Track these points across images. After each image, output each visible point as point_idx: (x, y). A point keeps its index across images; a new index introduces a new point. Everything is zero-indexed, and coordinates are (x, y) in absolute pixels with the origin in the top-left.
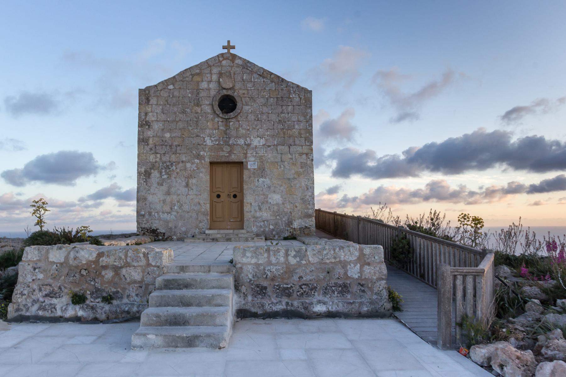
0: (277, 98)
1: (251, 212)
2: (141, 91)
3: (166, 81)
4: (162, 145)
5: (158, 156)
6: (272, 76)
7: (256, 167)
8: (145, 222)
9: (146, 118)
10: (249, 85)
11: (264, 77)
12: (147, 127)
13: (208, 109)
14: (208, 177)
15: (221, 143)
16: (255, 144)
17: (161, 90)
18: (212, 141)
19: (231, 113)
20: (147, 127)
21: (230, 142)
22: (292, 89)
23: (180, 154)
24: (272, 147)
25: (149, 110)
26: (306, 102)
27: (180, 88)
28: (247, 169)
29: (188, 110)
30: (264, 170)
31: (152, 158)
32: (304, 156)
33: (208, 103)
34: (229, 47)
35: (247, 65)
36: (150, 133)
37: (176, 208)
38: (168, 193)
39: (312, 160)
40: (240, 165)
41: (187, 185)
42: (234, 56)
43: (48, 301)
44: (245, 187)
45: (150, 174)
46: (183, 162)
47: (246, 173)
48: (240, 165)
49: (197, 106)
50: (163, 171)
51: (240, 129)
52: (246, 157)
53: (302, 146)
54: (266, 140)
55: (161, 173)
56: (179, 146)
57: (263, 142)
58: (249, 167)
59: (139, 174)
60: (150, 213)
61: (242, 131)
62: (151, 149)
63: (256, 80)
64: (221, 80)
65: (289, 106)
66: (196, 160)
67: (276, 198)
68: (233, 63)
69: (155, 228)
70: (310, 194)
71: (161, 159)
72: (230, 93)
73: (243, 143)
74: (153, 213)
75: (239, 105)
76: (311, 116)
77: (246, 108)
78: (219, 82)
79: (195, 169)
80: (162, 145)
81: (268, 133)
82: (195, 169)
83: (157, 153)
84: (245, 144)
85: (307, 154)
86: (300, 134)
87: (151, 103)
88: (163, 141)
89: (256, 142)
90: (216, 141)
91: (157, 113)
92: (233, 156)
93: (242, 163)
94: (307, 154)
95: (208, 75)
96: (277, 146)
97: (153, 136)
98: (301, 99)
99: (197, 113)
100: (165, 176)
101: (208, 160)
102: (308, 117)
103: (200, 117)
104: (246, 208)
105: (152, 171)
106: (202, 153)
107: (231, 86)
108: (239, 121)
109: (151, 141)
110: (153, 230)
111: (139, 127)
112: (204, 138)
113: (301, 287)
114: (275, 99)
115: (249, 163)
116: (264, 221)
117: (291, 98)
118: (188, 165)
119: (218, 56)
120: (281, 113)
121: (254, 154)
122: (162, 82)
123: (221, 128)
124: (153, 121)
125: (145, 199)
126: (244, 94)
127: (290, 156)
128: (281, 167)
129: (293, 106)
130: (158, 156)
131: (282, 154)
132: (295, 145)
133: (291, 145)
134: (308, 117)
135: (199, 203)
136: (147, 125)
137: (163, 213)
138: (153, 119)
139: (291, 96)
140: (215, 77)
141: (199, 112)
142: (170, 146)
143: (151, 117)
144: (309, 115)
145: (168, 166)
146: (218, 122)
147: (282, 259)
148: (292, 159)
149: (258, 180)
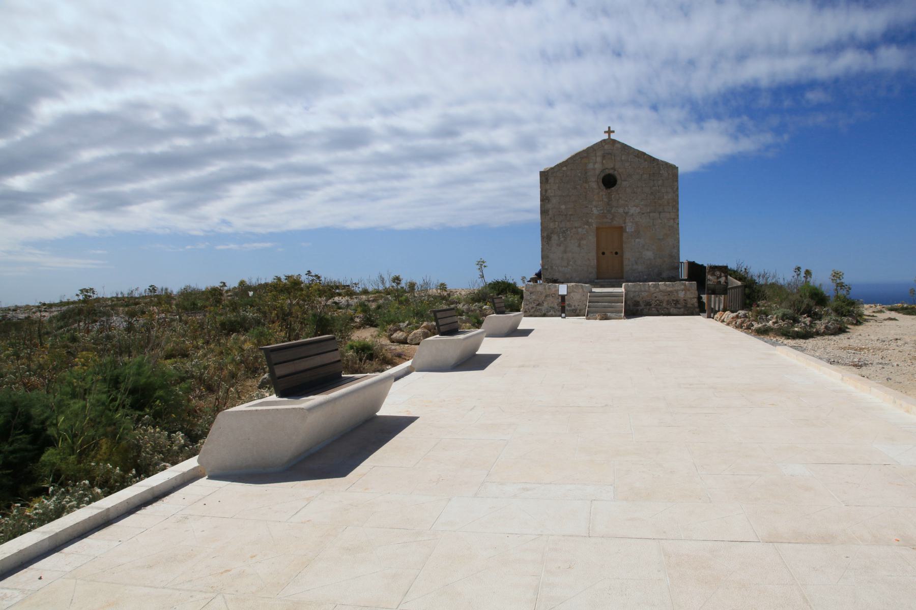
0: (650, 174)
1: (629, 265)
2: (541, 172)
3: (560, 164)
4: (559, 215)
5: (557, 223)
6: (645, 157)
7: (633, 230)
8: (548, 274)
9: (546, 194)
10: (627, 164)
11: (638, 157)
13: (594, 185)
14: (595, 239)
15: (605, 212)
16: (632, 212)
17: (557, 172)
18: (598, 211)
19: (613, 188)
20: (547, 201)
21: (612, 211)
22: (661, 166)
23: (573, 221)
24: (646, 214)
25: (548, 187)
26: (673, 176)
27: (572, 169)
28: (626, 232)
29: (578, 187)
30: (639, 232)
31: (552, 225)
32: (672, 221)
33: (594, 180)
34: (609, 132)
35: (625, 148)
36: (549, 206)
37: (571, 263)
38: (565, 252)
39: (678, 224)
41: (579, 246)
42: (614, 141)
43: (538, 307)
44: (624, 246)
45: (551, 237)
46: (575, 228)
47: (625, 235)
48: (621, 229)
49: (586, 183)
50: (561, 235)
51: (620, 200)
52: (625, 223)
53: (670, 212)
54: (641, 209)
55: (559, 237)
56: (572, 215)
57: (638, 210)
59: (543, 238)
60: (552, 267)
61: (621, 202)
62: (551, 218)
63: (632, 160)
64: (604, 161)
65: (659, 180)
66: (586, 226)
67: (649, 254)
68: (613, 146)
70: (676, 251)
71: (558, 226)
72: (611, 172)
73: (622, 212)
74: (554, 267)
75: (619, 182)
76: (678, 188)
77: (624, 183)
78: (603, 163)
79: (585, 232)
80: (559, 215)
81: (643, 203)
82: (585, 232)
83: (555, 221)
84: (624, 212)
85: (674, 219)
86: (668, 203)
87: (550, 181)
88: (559, 212)
89: (633, 210)
90: (601, 210)
91: (554, 190)
92: (615, 222)
93: (622, 227)
94: (674, 219)
95: (594, 158)
96: (649, 213)
98: (669, 174)
99: (585, 188)
100: (562, 239)
101: (594, 226)
102: (675, 189)
103: (588, 192)
104: (626, 262)
105: (552, 235)
106: (590, 220)
107: (612, 166)
108: (619, 194)
109: (550, 212)
110: (555, 280)
111: (541, 201)
112: (592, 208)
113: (656, 301)
114: (648, 175)
115: (627, 227)
117: (660, 174)
118: (580, 230)
119: (601, 141)
120: (654, 186)
121: (631, 220)
122: (558, 165)
123: (606, 200)
124: (551, 196)
125: (548, 257)
127: (660, 221)
128: (653, 230)
129: (663, 180)
130: (557, 223)
131: (653, 219)
132: (664, 212)
133: (661, 212)
134: (675, 189)
135: (589, 259)
136: (547, 199)
137: (562, 267)
138: (552, 195)
139: (661, 172)
140: (599, 159)
141: (587, 187)
142: (566, 215)
143: (550, 193)
144: (676, 187)
145: (564, 231)
146: (602, 195)
147: (647, 289)
148: (661, 223)
149: (635, 241)
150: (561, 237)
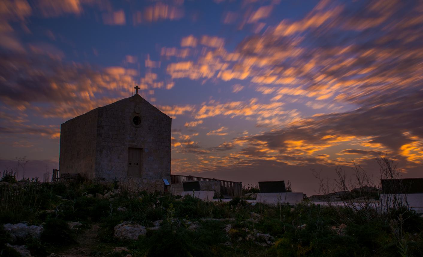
12: (101, 128)
15: (134, 139)
37: (113, 168)
40: (141, 149)
46: (117, 146)
50: (108, 150)
58: (145, 151)
64: (135, 109)
69: (104, 178)
93: (142, 149)
97: (104, 133)
98: (167, 121)
100: (109, 153)
114: (157, 120)
116: (150, 176)
126: (144, 116)
129: (164, 124)
149: (149, 157)
150: (108, 151)
